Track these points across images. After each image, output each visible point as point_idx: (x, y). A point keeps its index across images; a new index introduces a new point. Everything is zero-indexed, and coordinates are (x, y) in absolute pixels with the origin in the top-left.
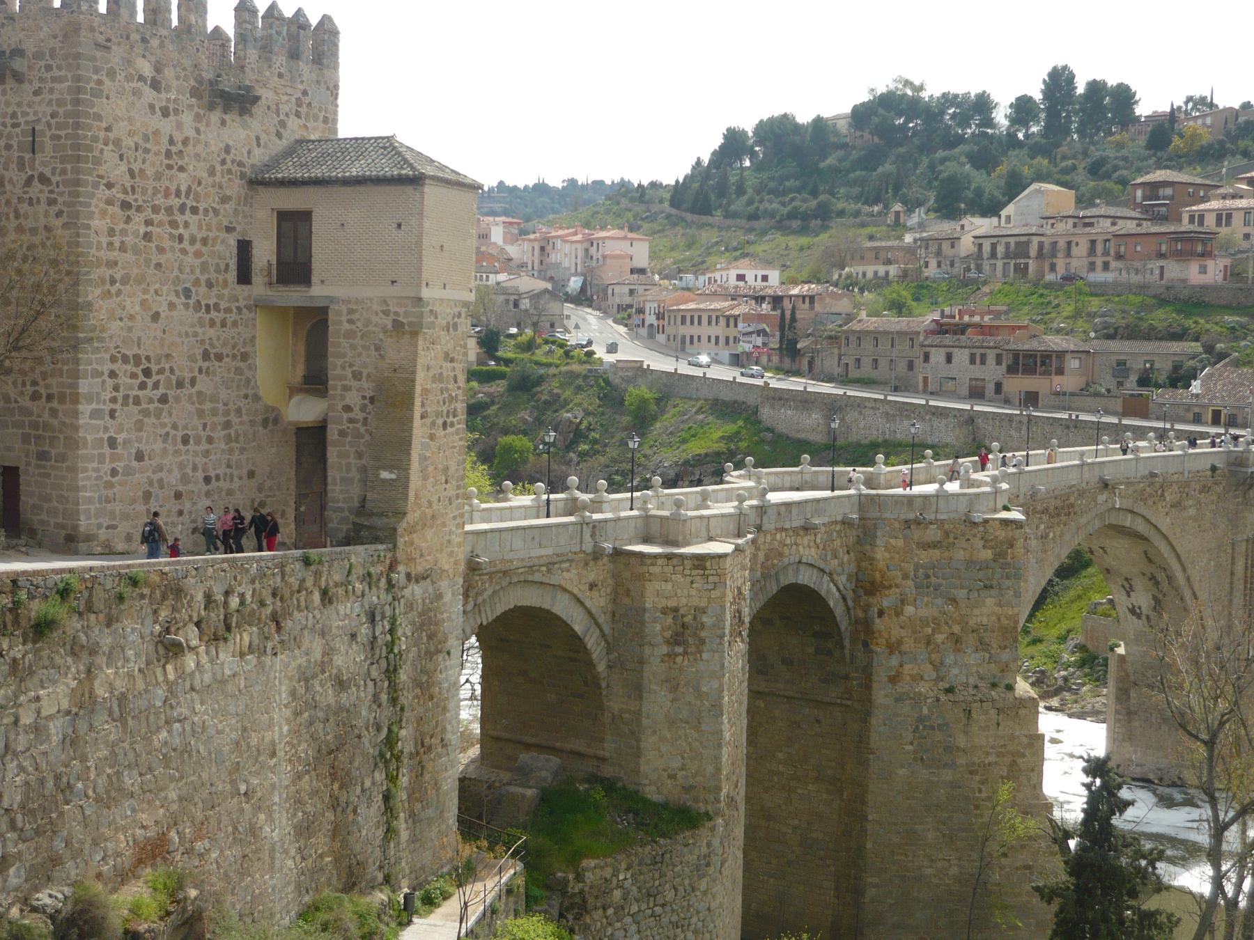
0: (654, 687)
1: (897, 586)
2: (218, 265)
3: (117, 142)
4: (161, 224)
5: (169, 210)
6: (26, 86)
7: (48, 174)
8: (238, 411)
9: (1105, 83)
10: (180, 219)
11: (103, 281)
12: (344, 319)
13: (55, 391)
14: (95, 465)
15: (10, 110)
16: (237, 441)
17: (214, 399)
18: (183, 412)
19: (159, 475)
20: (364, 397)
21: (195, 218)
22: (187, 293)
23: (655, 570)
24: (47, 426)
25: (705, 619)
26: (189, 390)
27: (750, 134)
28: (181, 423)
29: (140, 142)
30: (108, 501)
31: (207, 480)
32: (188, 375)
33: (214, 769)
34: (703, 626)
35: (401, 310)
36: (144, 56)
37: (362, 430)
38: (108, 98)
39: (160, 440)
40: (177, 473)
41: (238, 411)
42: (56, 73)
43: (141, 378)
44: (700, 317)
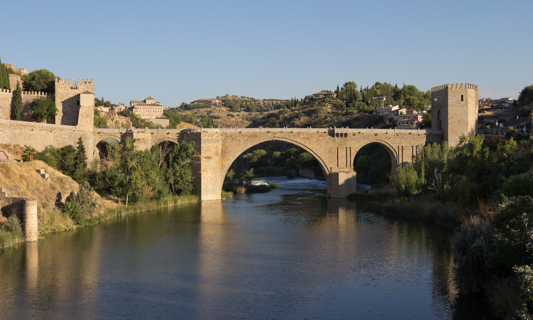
22: (70, 106)
26: (70, 115)
32: (70, 114)
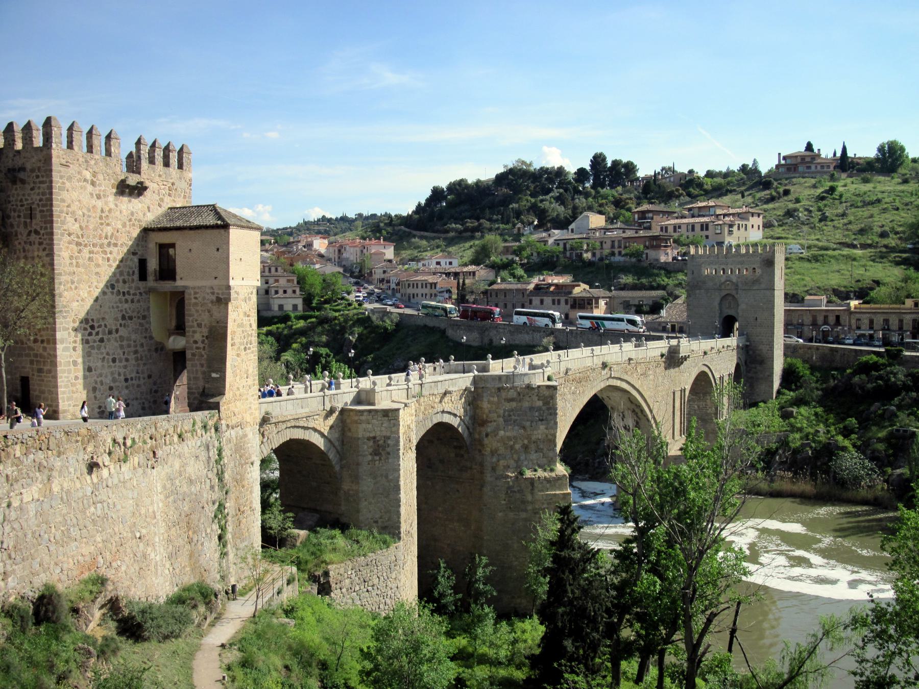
0: (364, 477)
1: (495, 421)
2: (128, 272)
3: (73, 213)
4: (98, 253)
5: (102, 246)
6: (27, 186)
7: (39, 230)
8: (142, 345)
9: (621, 161)
10: (108, 250)
11: (68, 282)
12: (192, 297)
13: (45, 338)
14: (66, 375)
15: (19, 198)
16: (141, 359)
17: (129, 339)
18: (112, 346)
19: (100, 379)
20: (203, 336)
21: (116, 249)
23: (363, 418)
24: (41, 356)
25: (389, 442)
26: (114, 335)
27: (445, 189)
28: (111, 352)
29: (86, 212)
30: (73, 392)
31: (126, 380)
32: (114, 328)
33: (121, 526)
34: (388, 445)
35: (220, 292)
36: (87, 170)
37: (203, 353)
38: (68, 191)
39: (100, 361)
40: (110, 378)
41: (142, 345)
42: (41, 179)
43: (89, 330)
44: (417, 284)
